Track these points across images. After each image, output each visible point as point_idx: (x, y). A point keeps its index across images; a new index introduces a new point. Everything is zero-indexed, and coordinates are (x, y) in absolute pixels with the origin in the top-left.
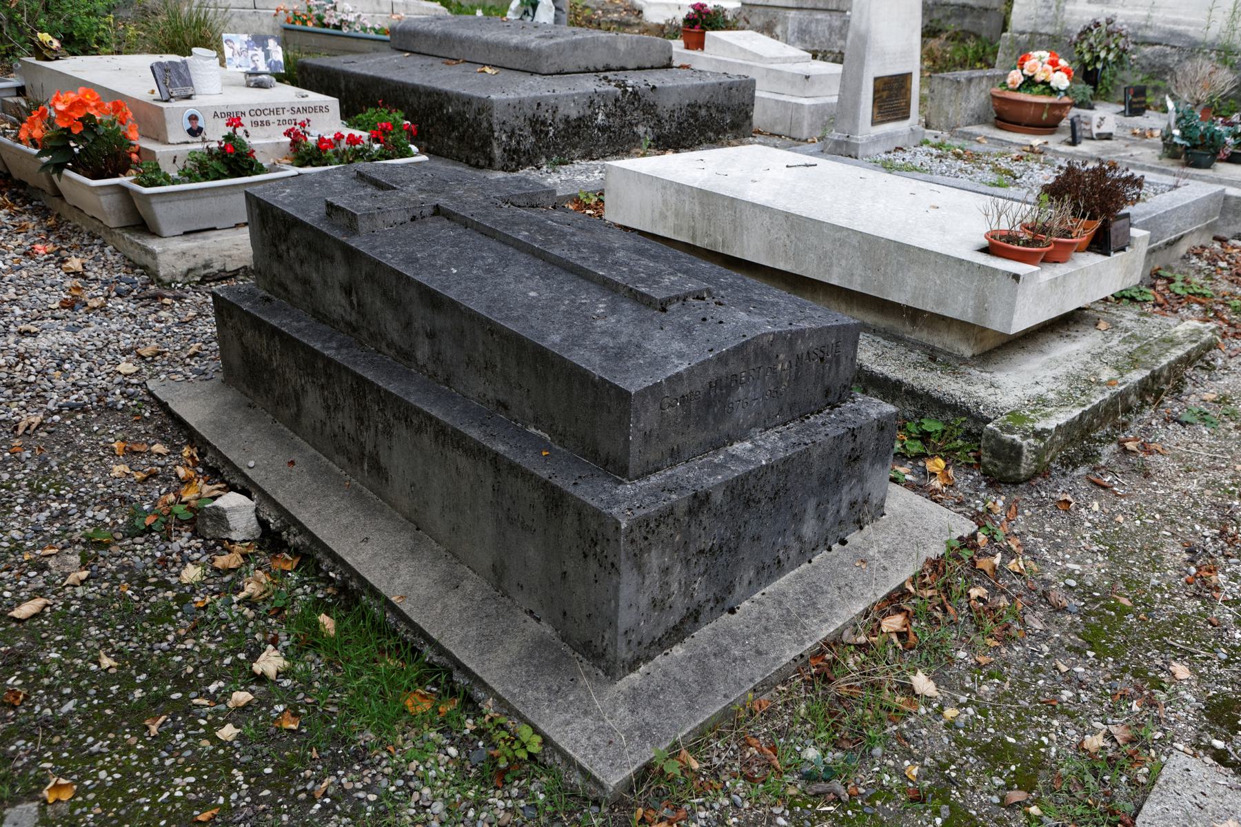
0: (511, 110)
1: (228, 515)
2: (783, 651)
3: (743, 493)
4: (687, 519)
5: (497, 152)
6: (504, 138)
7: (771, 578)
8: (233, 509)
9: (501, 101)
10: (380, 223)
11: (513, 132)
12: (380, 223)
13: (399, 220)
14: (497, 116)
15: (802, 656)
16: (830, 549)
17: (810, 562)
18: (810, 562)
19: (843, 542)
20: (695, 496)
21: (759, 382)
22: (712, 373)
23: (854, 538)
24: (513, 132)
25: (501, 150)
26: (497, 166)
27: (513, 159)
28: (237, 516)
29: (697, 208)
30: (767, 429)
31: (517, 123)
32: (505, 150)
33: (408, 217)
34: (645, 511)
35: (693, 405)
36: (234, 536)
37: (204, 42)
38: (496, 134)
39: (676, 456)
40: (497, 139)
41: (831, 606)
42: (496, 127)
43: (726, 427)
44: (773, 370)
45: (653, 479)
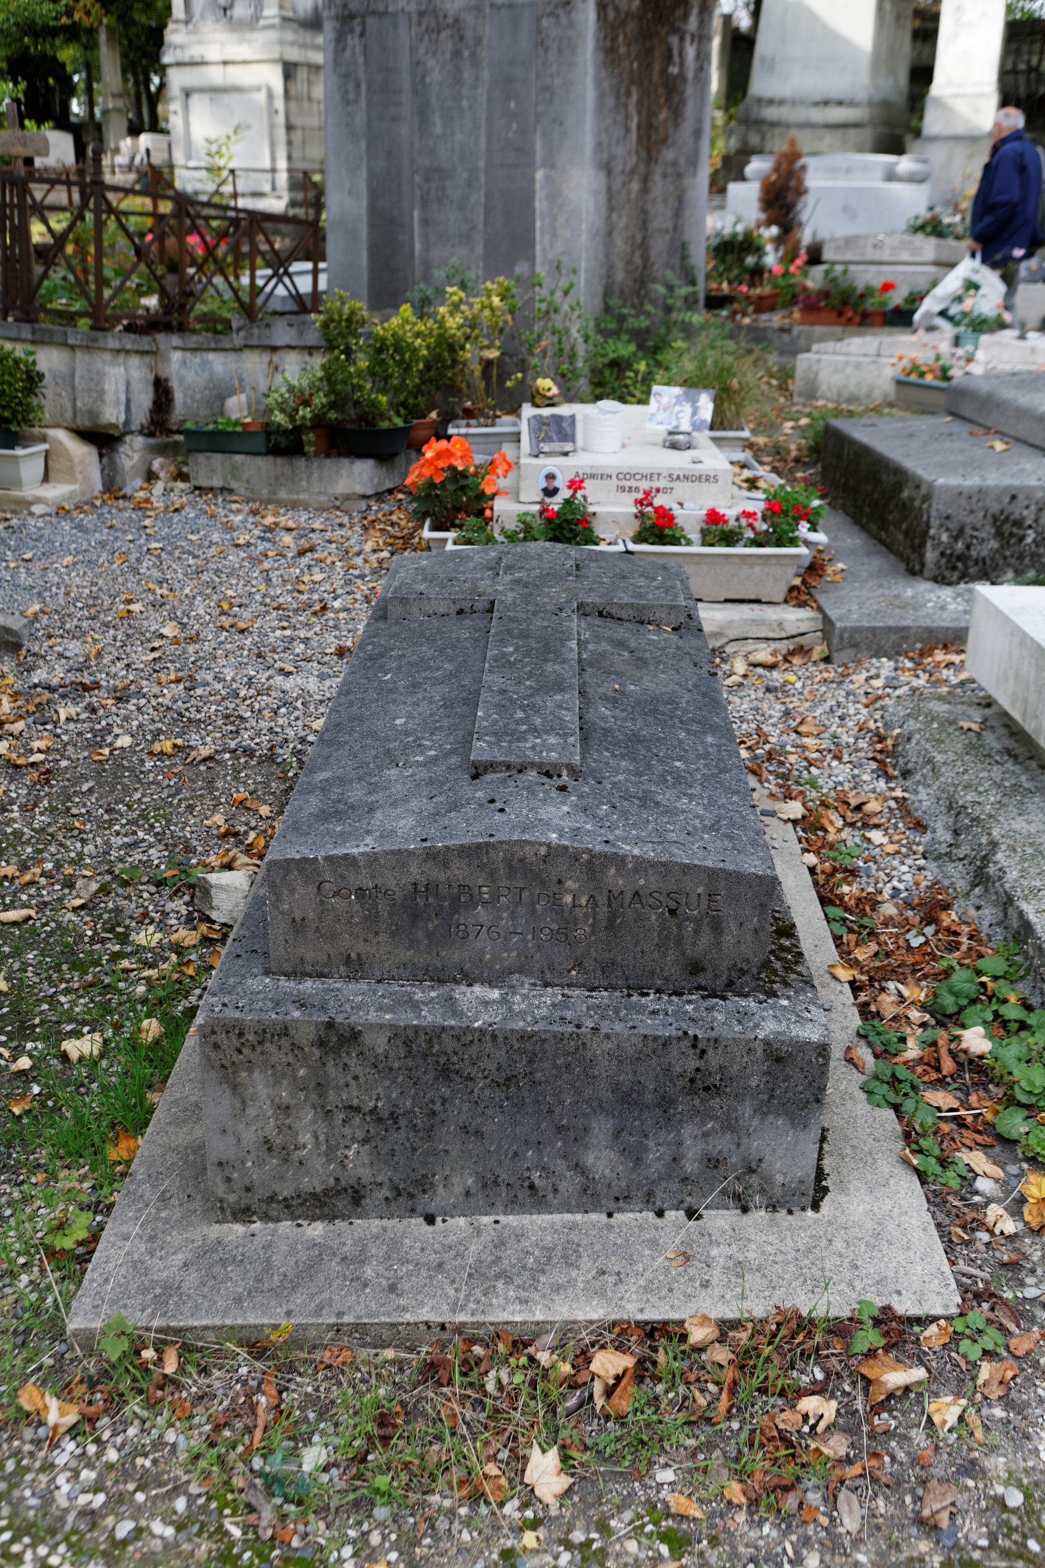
0: (963, 501)
1: (213, 891)
2: (422, 1304)
3: (435, 1058)
4: (317, 1052)
5: (930, 556)
6: (944, 537)
7: (513, 1205)
8: (221, 888)
9: (947, 489)
10: (415, 610)
11: (961, 531)
12: (415, 610)
13: (441, 610)
14: (937, 507)
15: (443, 1327)
16: (660, 1214)
17: (610, 1215)
18: (610, 1215)
19: (692, 1214)
20: (330, 1025)
21: (521, 910)
22: (415, 871)
23: (720, 1220)
24: (961, 531)
25: (937, 553)
26: (926, 574)
27: (954, 568)
28: (224, 896)
29: (1033, 671)
30: (546, 985)
31: (969, 520)
32: (942, 554)
33: (453, 609)
34: (237, 1014)
35: (383, 908)
36: (214, 915)
37: (222, 399)
38: (932, 532)
39: (355, 968)
40: (933, 538)
41: (557, 1288)
42: (935, 523)
43: (455, 955)
44: (555, 901)
45: (308, 985)
